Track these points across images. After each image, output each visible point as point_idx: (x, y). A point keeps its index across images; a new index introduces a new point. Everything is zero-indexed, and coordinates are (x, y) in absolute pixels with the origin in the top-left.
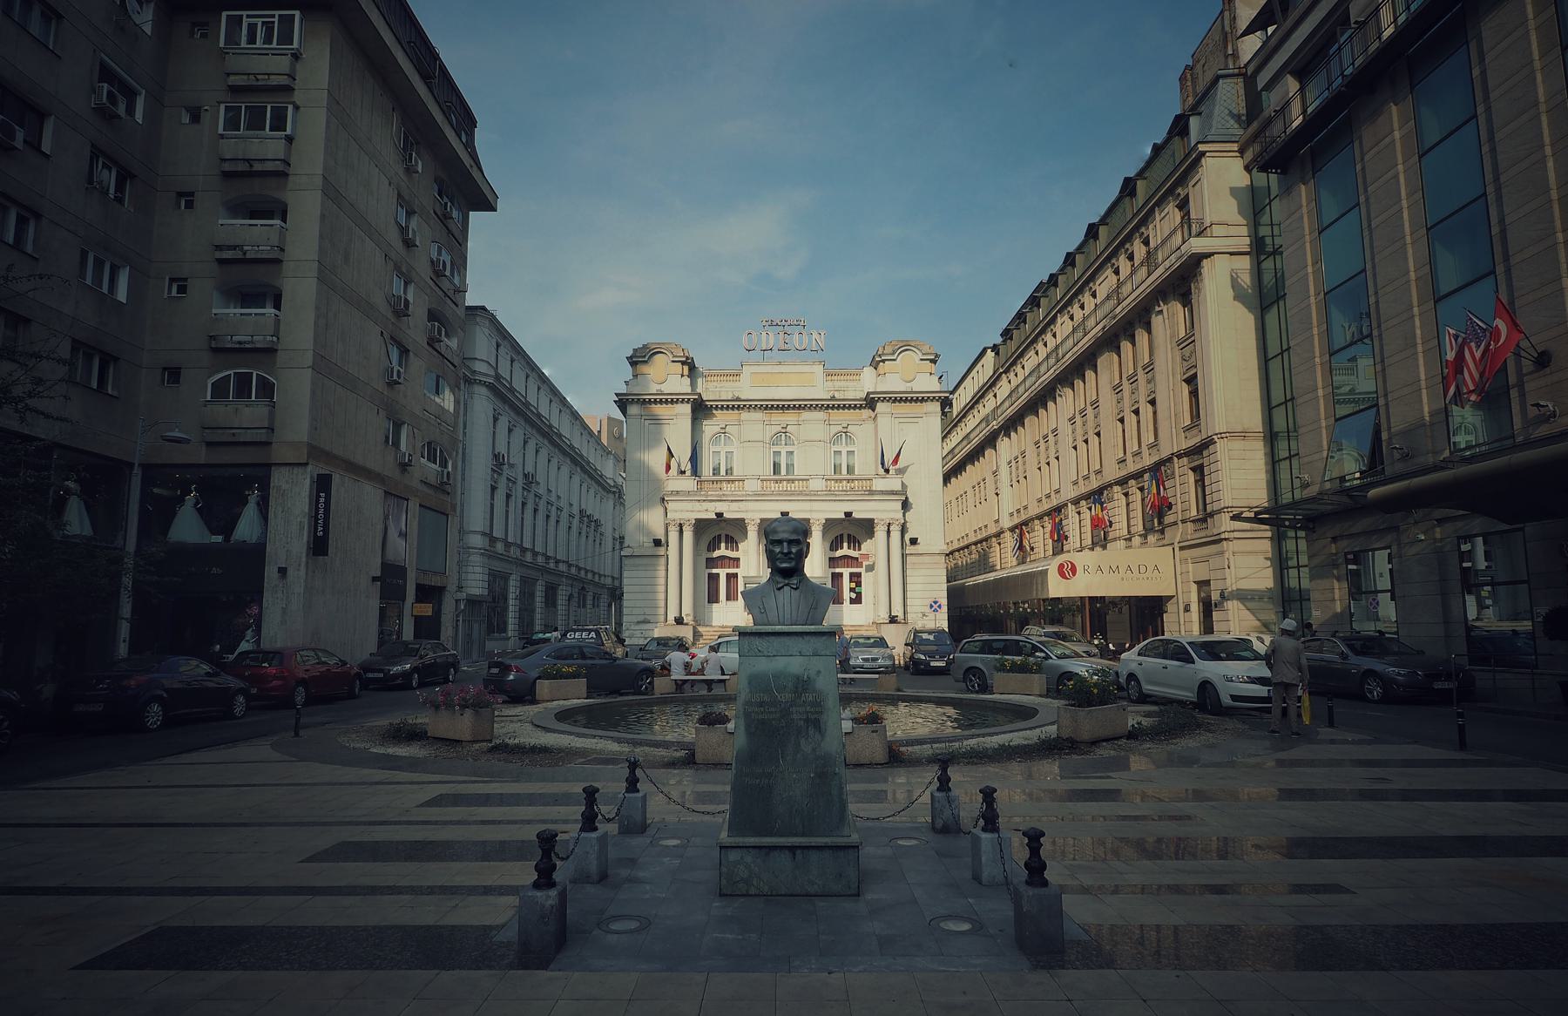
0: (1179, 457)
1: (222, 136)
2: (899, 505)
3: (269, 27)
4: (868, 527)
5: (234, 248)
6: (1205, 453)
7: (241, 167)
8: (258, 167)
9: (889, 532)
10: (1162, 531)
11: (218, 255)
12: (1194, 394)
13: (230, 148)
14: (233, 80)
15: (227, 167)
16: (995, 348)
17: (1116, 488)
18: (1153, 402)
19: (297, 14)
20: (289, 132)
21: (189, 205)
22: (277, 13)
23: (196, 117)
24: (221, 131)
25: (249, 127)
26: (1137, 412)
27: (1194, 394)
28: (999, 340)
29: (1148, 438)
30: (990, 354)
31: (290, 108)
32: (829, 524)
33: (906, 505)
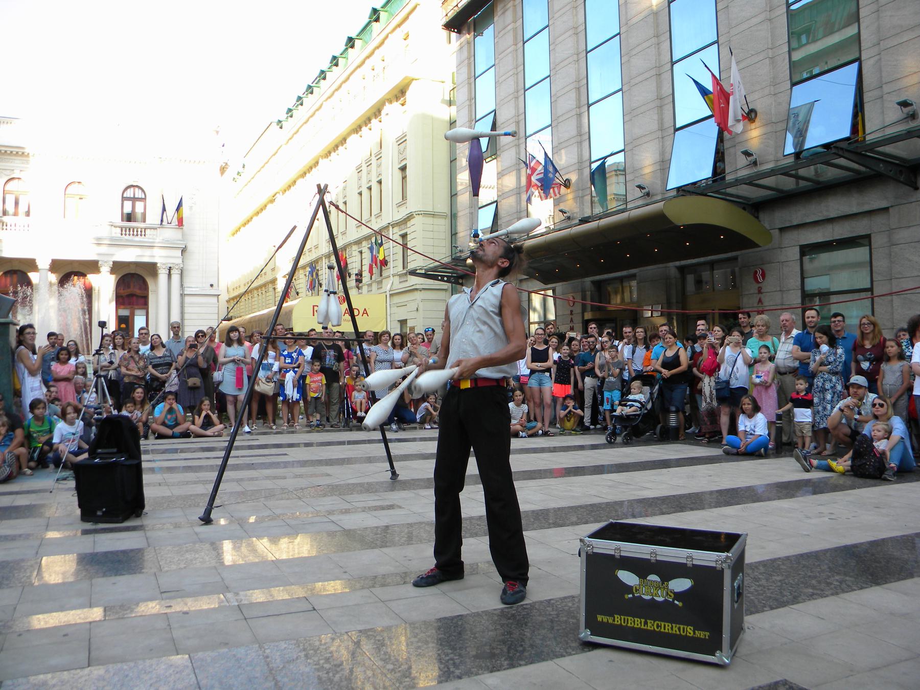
0: (393, 226)
2: (179, 253)
4: (152, 268)
6: (409, 224)
9: (170, 275)
10: (381, 282)
12: (404, 178)
17: (355, 247)
18: (380, 182)
26: (370, 188)
27: (404, 178)
28: (283, 117)
29: (375, 210)
30: (275, 127)
32: (117, 267)
33: (184, 251)
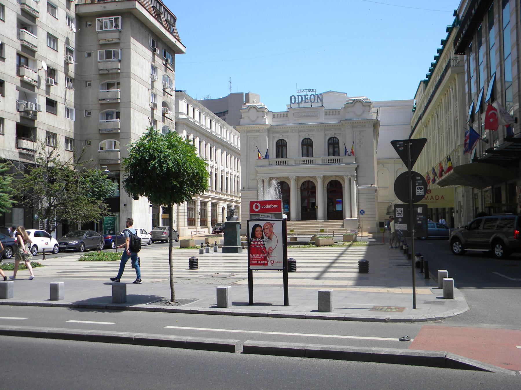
1: (99, 62)
3: (111, 23)
5: (104, 100)
7: (106, 72)
8: (111, 72)
11: (100, 102)
13: (101, 66)
14: (101, 42)
15: (101, 72)
16: (424, 82)
19: (120, 17)
20: (120, 58)
21: (90, 85)
22: (113, 17)
23: (90, 55)
24: (98, 60)
25: (107, 58)
31: (119, 49)
